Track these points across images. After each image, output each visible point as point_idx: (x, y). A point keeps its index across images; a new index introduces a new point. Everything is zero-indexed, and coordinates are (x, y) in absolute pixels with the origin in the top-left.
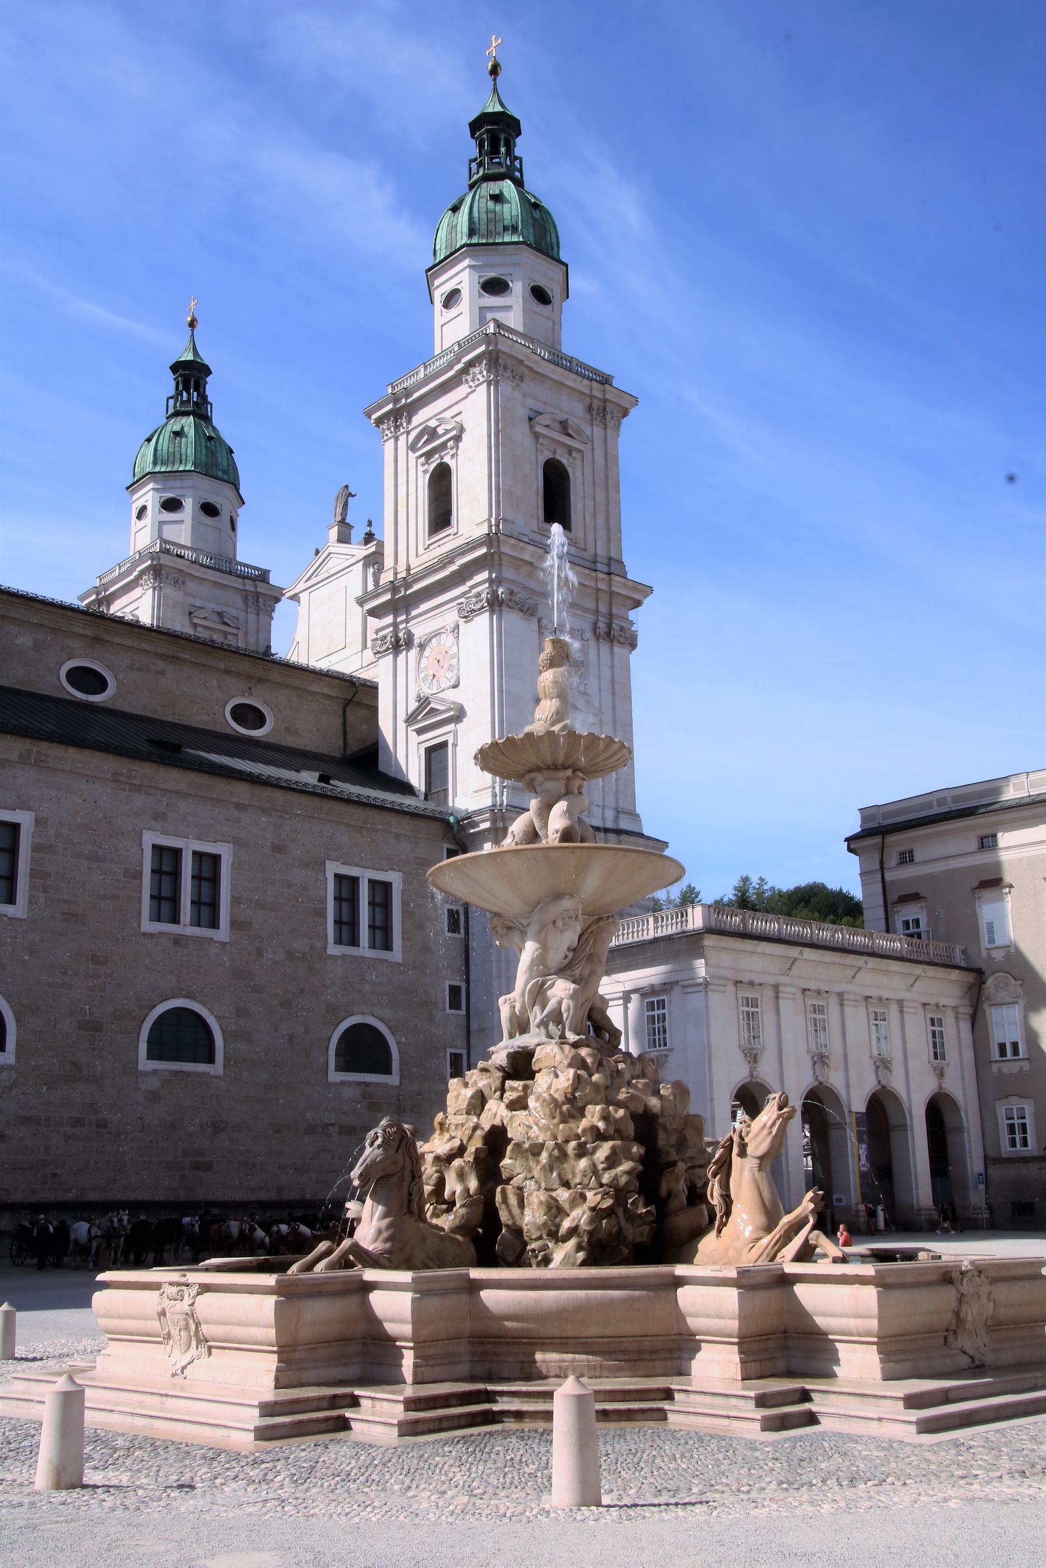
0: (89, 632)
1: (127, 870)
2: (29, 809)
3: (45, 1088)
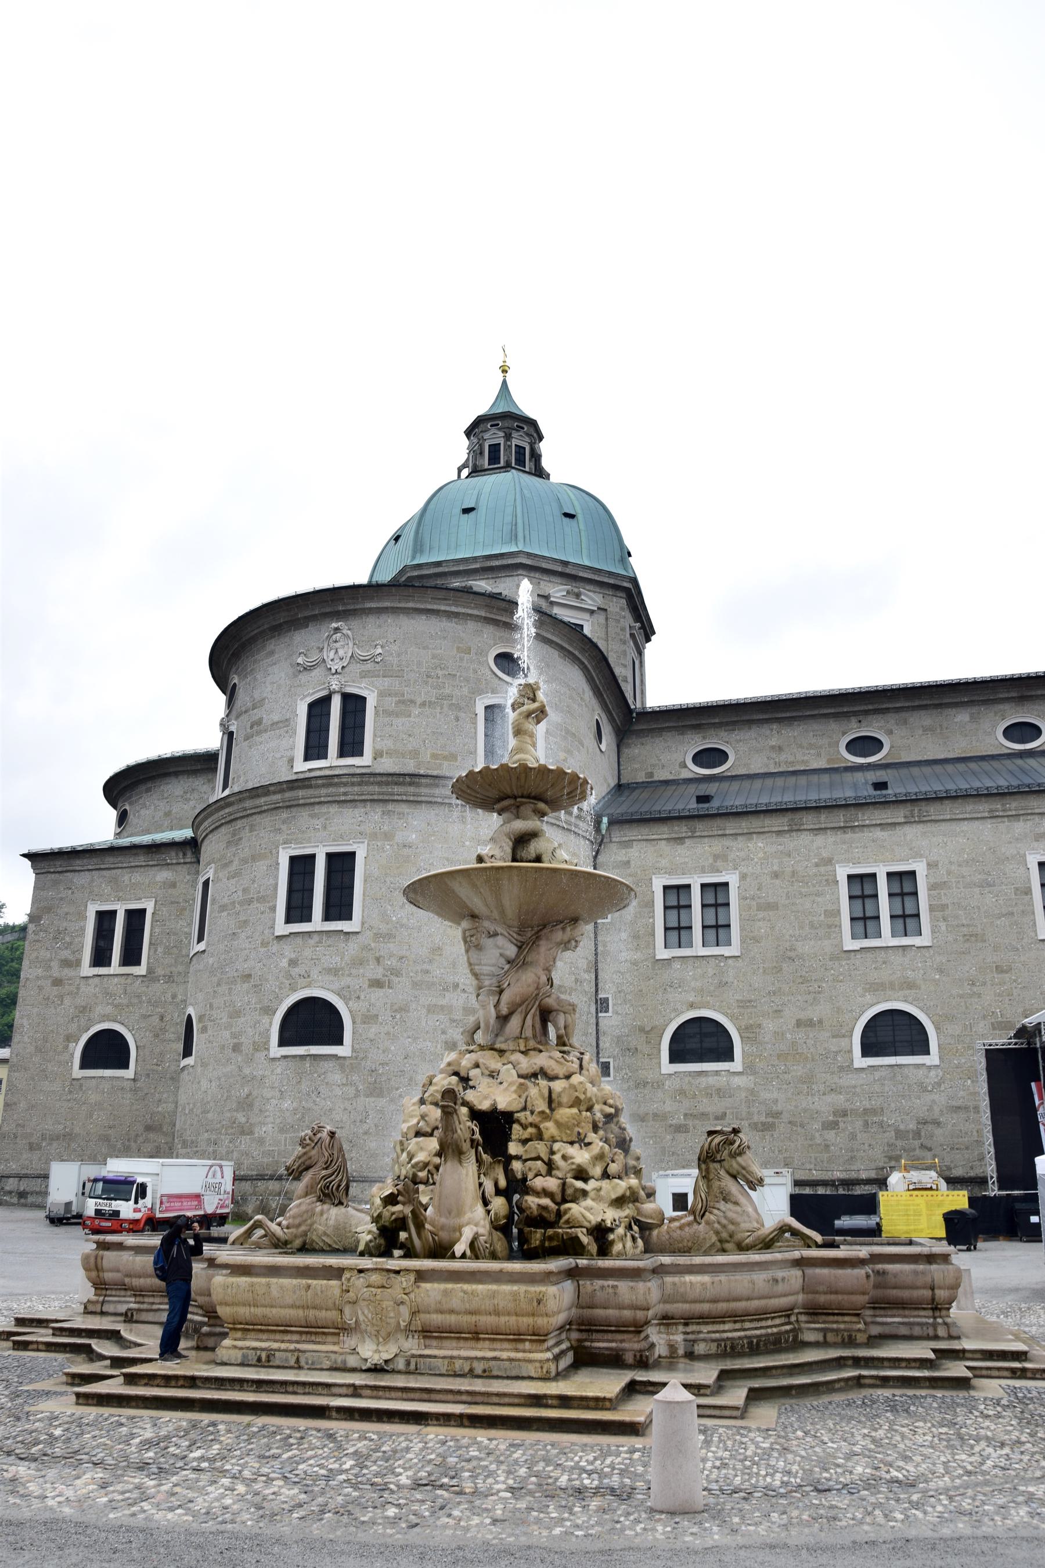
0: (1014, 695)
1: (1017, 889)
2: (921, 856)
3: (969, 1081)
